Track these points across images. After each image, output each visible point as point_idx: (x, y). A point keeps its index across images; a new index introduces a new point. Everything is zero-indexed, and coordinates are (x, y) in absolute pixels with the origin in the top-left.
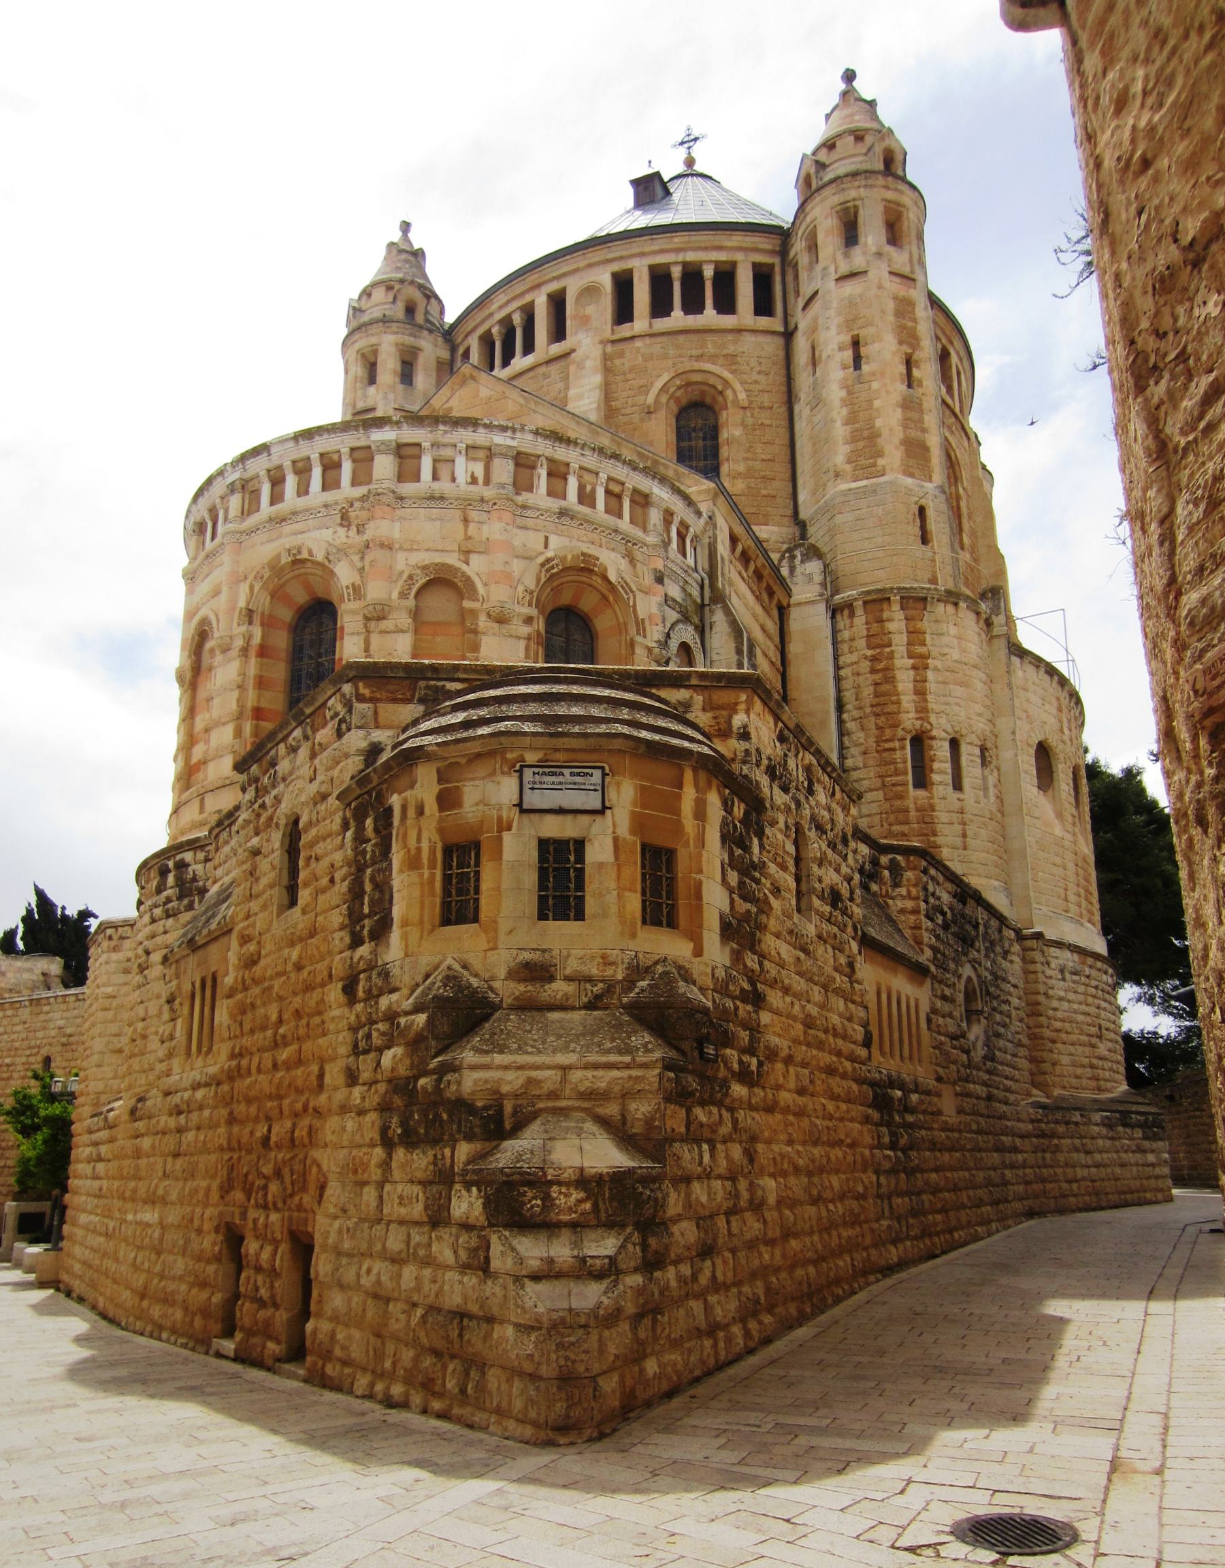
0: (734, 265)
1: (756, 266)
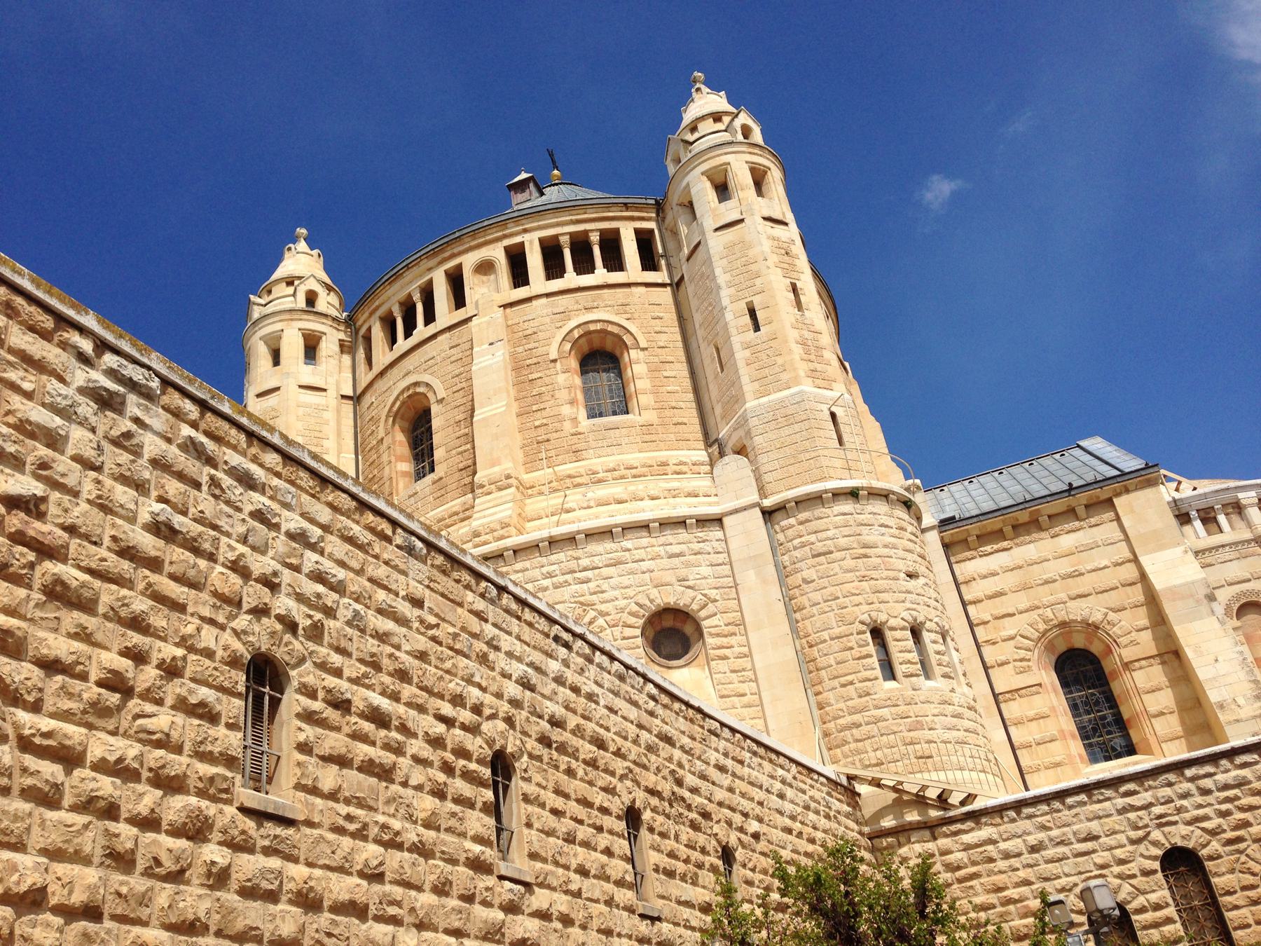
0: (616, 232)
1: (638, 232)
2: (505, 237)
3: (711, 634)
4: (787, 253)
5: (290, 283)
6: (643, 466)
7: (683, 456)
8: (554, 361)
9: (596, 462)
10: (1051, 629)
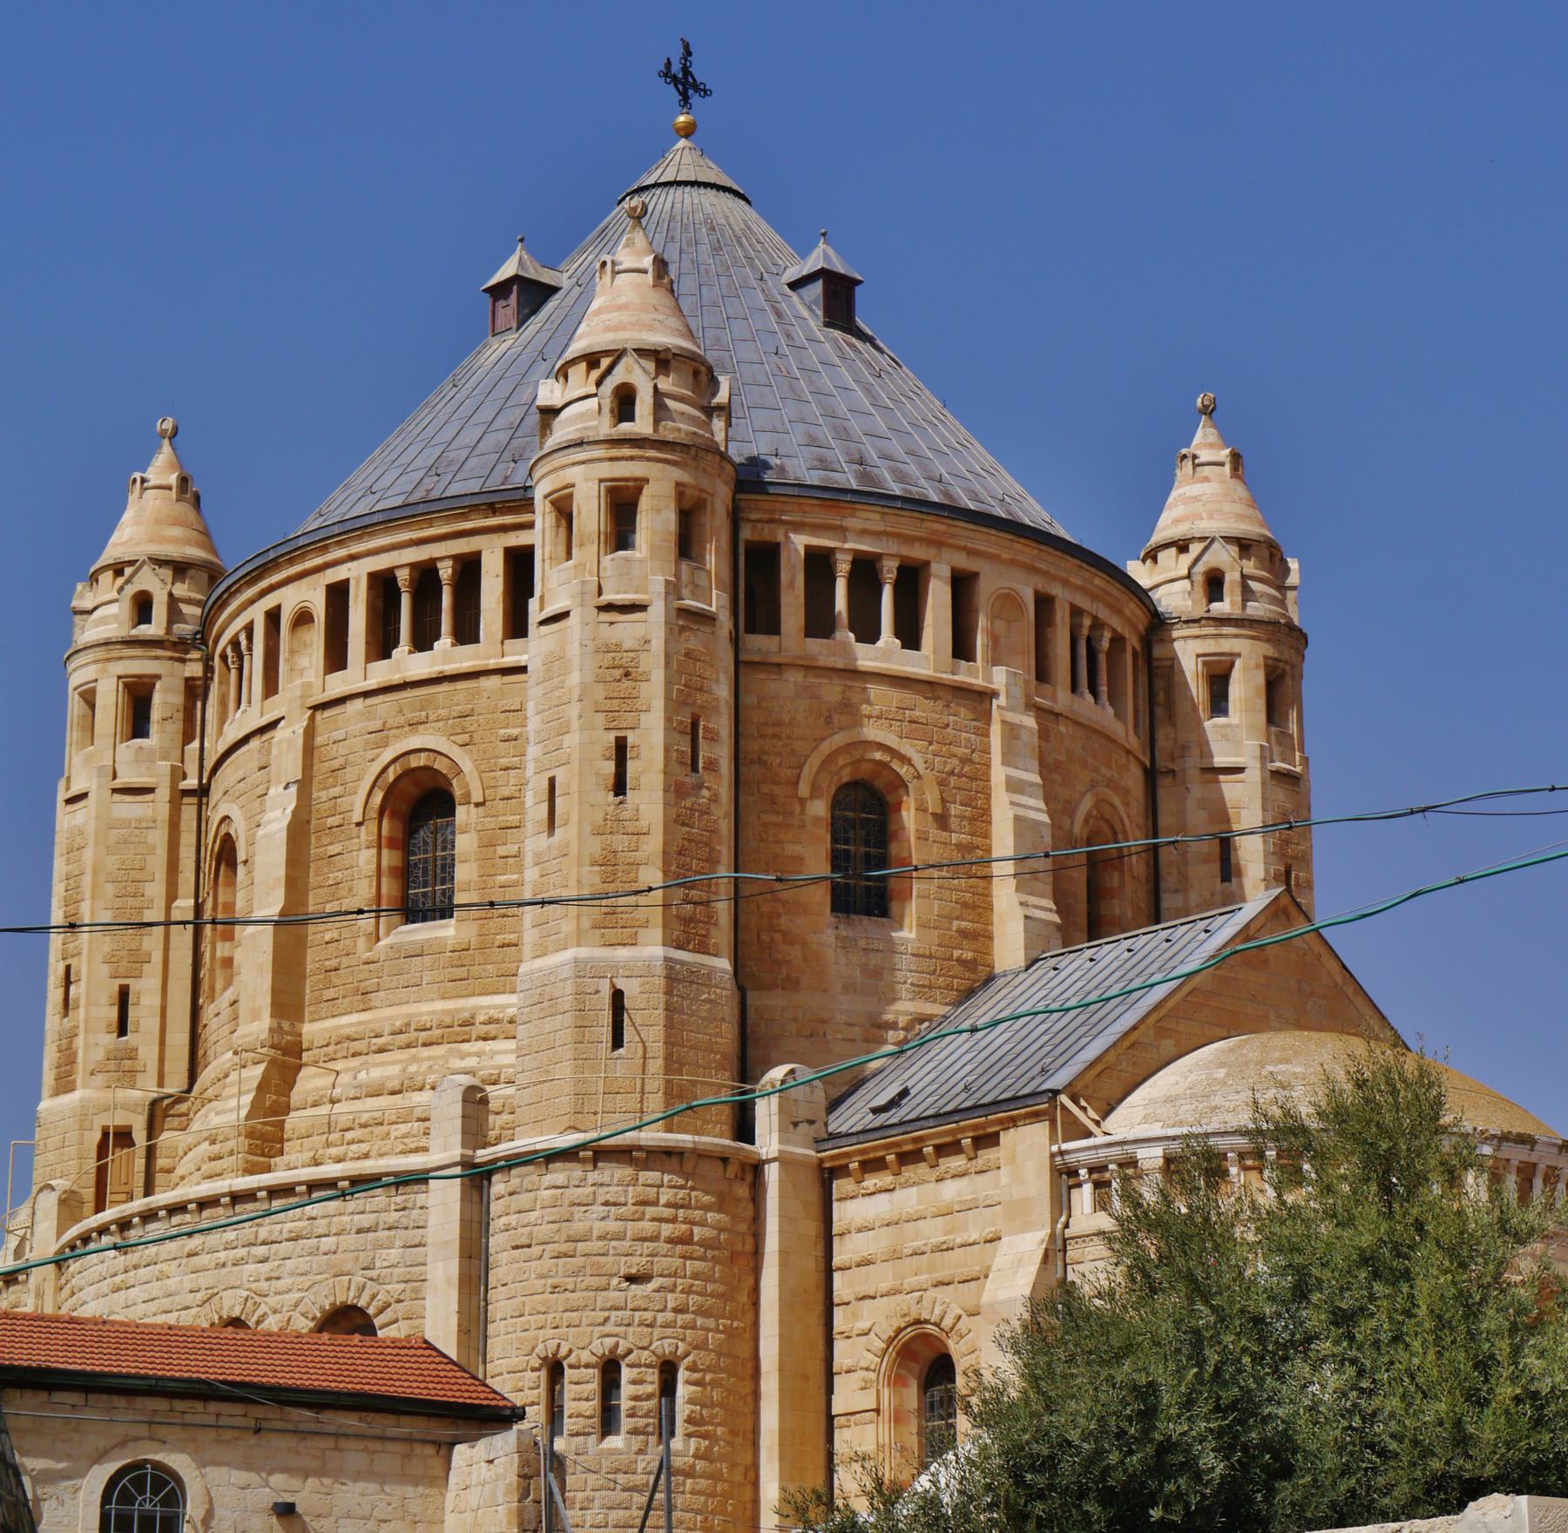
5: (119, 572)
6: (439, 1027)
7: (495, 1007)
8: (359, 824)
9: (386, 1015)
10: (906, 1328)
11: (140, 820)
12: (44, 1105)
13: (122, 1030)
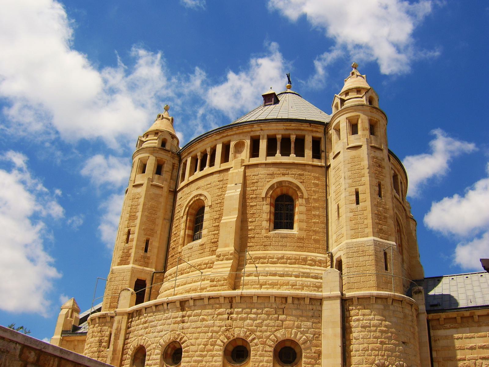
0: (304, 136)
1: (313, 137)
2: (252, 131)
3: (306, 357)
4: (379, 166)
7: (314, 256)
8: (263, 198)
11: (158, 194)
12: (115, 267)
13: (146, 251)
